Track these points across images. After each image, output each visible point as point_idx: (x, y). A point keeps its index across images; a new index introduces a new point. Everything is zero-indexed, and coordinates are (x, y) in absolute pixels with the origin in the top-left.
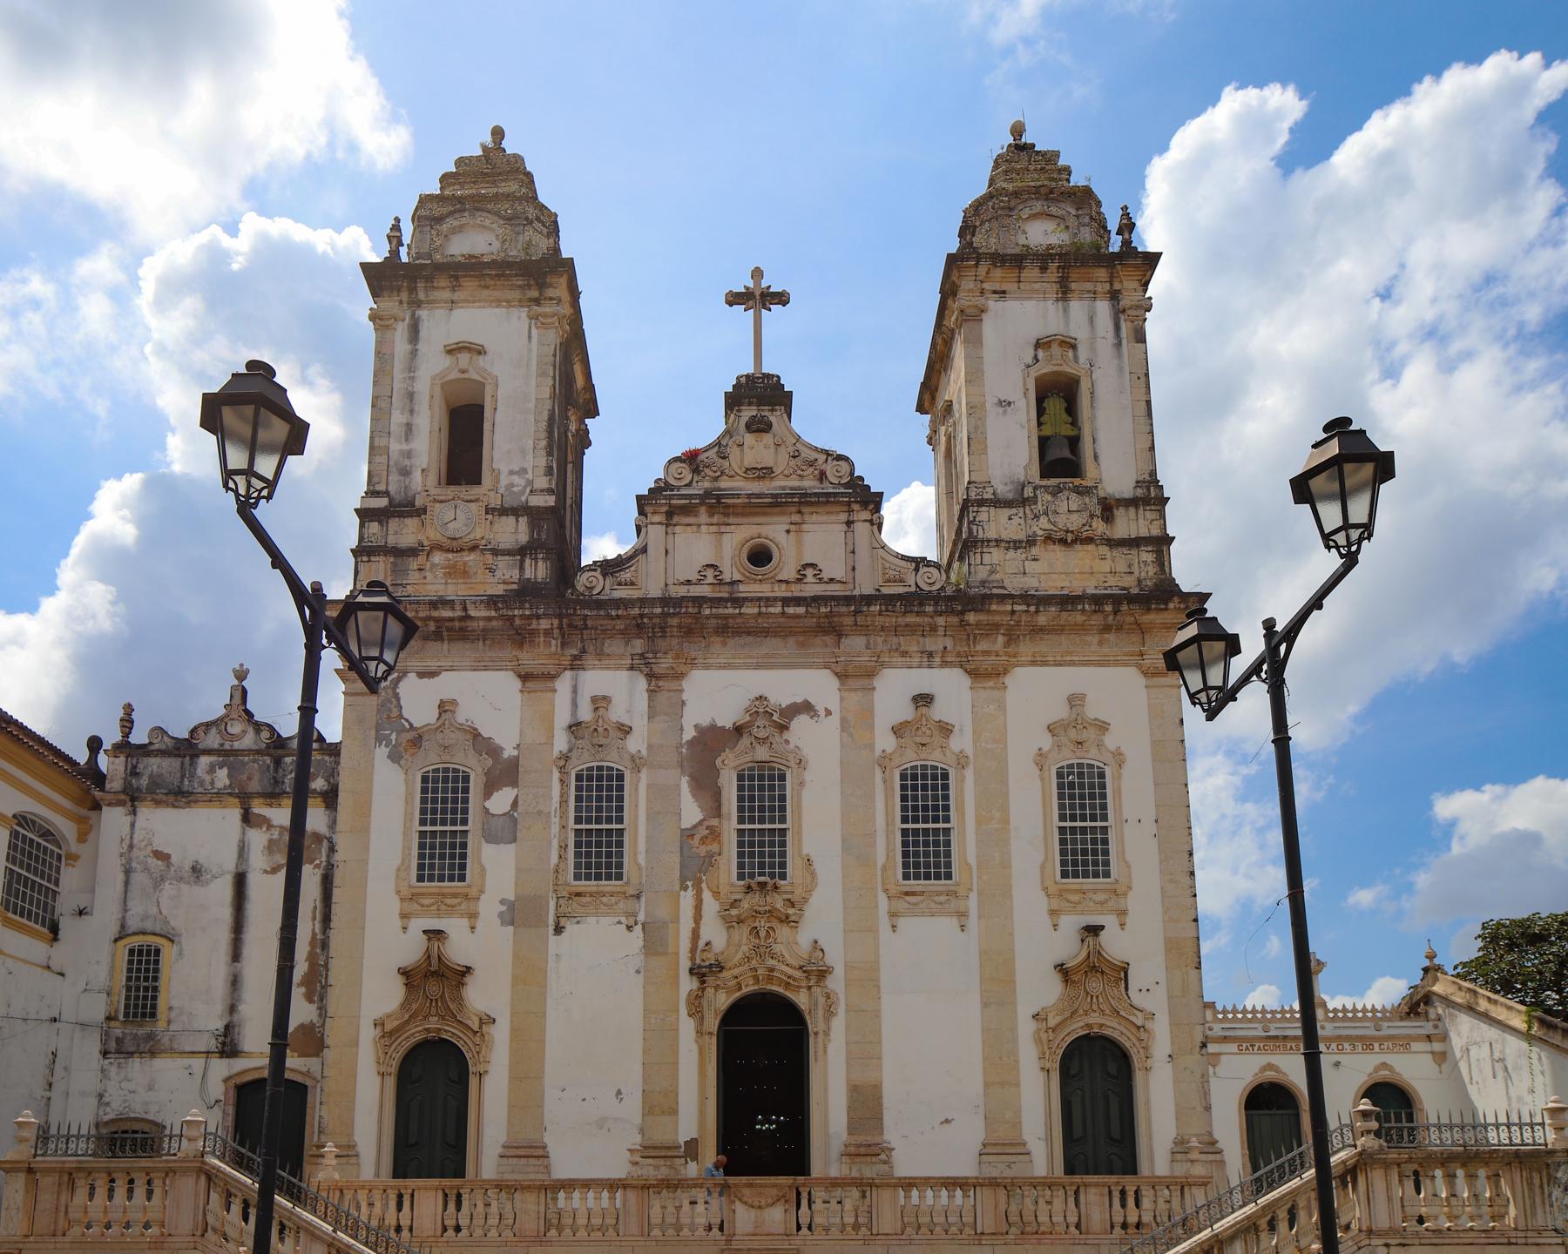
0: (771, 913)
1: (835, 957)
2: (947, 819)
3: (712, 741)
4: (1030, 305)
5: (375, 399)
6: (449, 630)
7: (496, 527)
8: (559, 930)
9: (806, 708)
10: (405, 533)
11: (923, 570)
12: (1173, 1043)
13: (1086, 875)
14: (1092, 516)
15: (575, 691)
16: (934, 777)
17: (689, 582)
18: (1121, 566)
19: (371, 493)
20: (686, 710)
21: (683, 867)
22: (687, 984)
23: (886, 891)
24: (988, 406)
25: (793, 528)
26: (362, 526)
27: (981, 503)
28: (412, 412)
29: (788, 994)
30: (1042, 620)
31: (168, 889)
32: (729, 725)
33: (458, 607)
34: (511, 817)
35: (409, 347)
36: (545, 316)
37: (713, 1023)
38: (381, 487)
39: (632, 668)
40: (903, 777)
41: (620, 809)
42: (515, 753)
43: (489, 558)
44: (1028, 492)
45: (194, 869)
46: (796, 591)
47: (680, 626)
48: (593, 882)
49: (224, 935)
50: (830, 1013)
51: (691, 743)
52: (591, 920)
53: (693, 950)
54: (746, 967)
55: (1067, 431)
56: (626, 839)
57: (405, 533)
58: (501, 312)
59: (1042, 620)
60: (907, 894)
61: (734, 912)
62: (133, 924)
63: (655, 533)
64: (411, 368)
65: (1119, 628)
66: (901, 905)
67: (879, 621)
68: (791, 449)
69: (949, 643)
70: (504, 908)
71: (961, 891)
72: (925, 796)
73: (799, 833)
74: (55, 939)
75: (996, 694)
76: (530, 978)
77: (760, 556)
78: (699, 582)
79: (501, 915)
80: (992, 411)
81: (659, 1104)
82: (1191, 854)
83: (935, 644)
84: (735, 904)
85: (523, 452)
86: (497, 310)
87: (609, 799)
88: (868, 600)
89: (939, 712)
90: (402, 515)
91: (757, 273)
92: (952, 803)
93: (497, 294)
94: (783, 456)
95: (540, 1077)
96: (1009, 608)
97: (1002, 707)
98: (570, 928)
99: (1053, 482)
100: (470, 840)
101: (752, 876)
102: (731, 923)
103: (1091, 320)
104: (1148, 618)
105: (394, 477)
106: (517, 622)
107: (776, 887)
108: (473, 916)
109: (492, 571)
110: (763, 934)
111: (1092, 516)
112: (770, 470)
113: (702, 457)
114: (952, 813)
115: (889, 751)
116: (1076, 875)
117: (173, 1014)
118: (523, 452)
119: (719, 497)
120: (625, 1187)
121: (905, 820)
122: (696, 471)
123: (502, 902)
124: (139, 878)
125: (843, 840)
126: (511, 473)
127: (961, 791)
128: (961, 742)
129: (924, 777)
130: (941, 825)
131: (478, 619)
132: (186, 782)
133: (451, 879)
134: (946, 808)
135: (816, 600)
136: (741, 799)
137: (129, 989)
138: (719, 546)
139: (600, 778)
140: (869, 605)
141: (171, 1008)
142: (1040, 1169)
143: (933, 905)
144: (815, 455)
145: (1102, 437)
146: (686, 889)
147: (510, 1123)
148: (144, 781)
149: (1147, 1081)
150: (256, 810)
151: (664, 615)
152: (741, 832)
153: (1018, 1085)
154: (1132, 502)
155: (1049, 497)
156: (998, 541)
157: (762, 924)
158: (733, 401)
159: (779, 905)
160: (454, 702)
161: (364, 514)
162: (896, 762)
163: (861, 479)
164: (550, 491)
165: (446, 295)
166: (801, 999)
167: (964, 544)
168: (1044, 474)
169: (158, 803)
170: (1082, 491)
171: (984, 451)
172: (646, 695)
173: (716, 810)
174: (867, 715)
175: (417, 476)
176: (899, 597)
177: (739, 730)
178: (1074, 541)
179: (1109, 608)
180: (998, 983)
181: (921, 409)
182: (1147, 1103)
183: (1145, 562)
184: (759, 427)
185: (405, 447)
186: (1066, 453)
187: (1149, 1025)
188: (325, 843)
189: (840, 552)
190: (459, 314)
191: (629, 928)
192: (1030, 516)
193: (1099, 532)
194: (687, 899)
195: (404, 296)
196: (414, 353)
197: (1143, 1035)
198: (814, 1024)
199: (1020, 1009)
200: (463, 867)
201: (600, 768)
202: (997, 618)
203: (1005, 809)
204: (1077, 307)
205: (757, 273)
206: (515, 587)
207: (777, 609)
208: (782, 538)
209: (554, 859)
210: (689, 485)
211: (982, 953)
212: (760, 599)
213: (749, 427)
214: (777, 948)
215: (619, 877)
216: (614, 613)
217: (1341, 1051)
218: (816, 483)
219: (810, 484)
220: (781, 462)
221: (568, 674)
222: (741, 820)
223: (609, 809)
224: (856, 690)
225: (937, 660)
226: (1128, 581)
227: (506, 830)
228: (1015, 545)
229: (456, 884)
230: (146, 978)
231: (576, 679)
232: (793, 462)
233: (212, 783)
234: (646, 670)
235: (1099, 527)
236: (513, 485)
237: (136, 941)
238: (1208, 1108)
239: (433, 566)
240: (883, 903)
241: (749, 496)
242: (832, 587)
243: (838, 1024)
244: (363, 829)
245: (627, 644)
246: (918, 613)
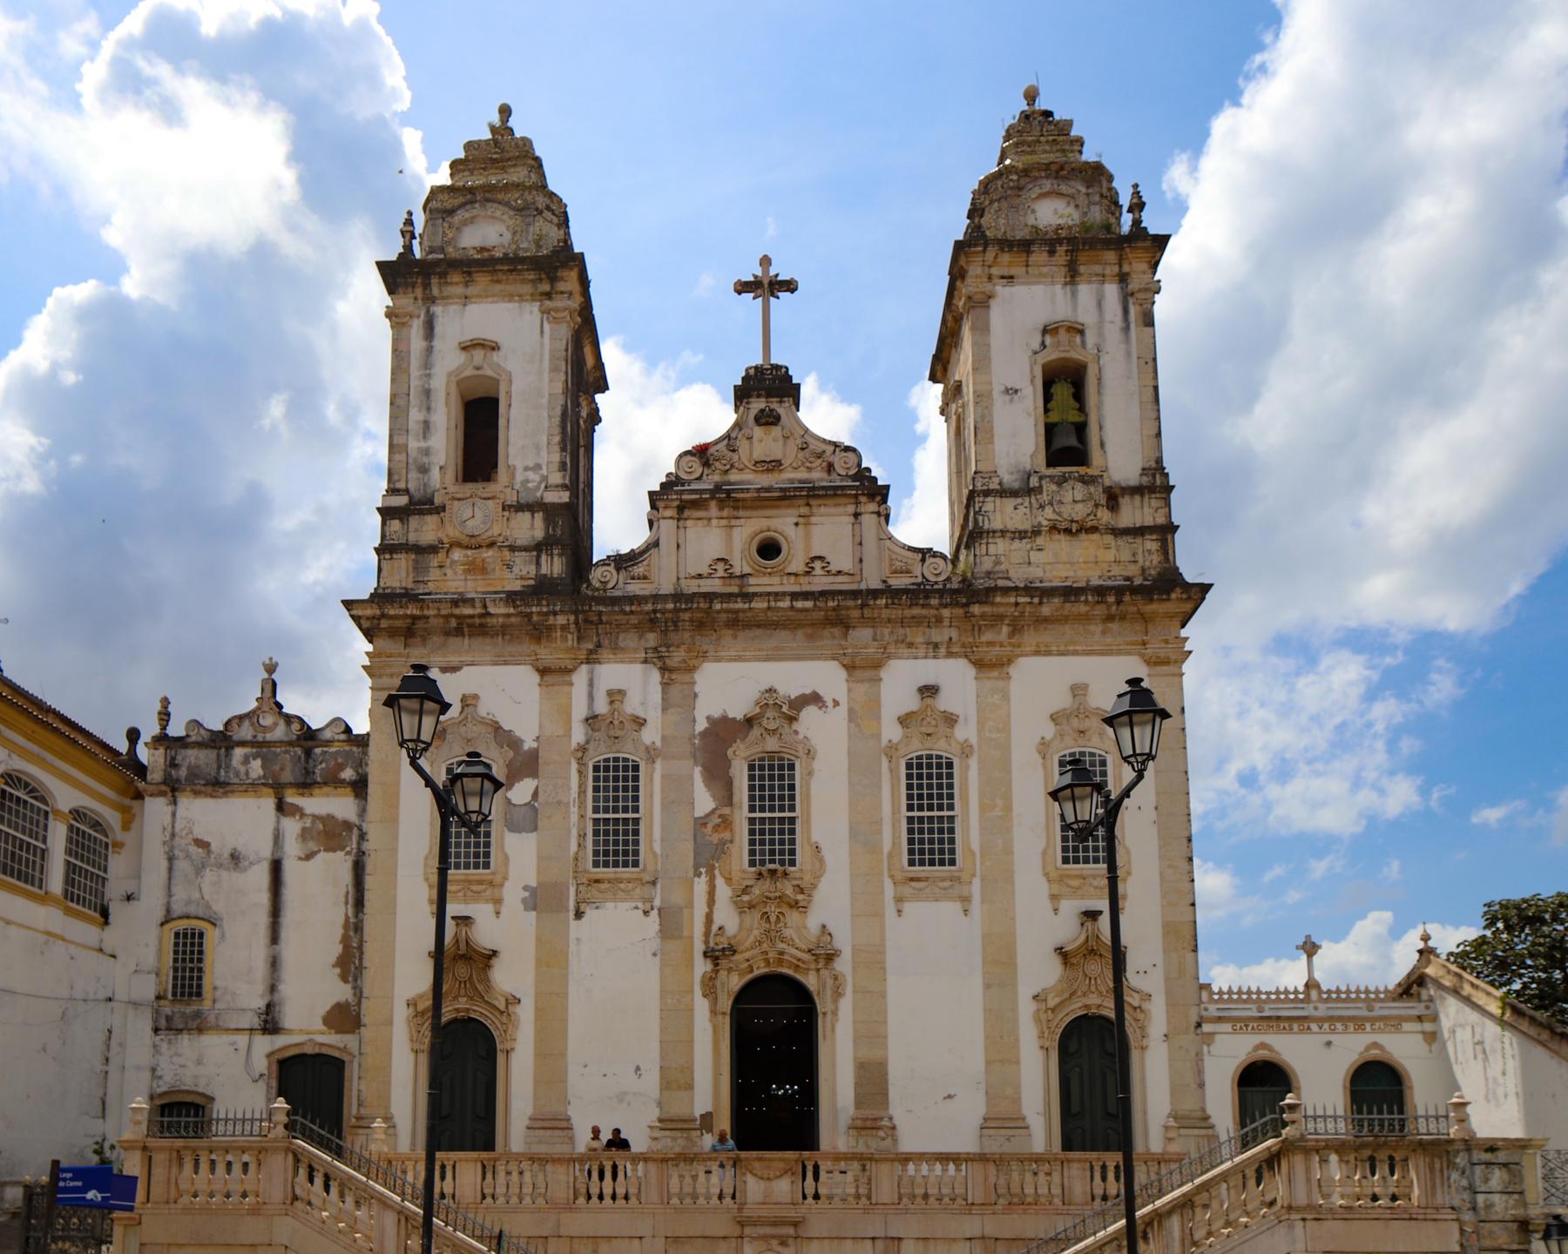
0: (781, 899)
1: (843, 941)
2: (951, 807)
3: (723, 732)
4: (1038, 290)
5: (394, 397)
6: (469, 626)
7: (513, 522)
8: (579, 915)
9: (815, 699)
10: (425, 530)
11: (929, 561)
12: (1169, 1022)
13: (1086, 861)
14: (1097, 506)
15: (591, 684)
16: (939, 766)
17: (700, 576)
18: (1126, 555)
19: (392, 491)
20: (699, 702)
21: (697, 854)
22: (702, 967)
23: (892, 877)
24: (996, 394)
25: (801, 520)
26: (384, 524)
27: (987, 493)
28: (429, 409)
29: (798, 977)
30: (1046, 610)
31: (209, 875)
32: (739, 716)
33: (478, 604)
34: (531, 807)
35: (424, 344)
36: (557, 310)
37: (726, 1004)
38: (401, 485)
39: (645, 661)
40: (909, 766)
41: (636, 799)
42: (535, 745)
43: (507, 553)
44: (1034, 482)
45: (232, 856)
46: (806, 585)
47: (691, 621)
48: (611, 869)
49: (263, 919)
50: (838, 994)
51: (704, 734)
52: (610, 905)
53: (707, 934)
54: (757, 951)
55: (1074, 417)
56: (642, 827)
57: (425, 530)
58: (513, 306)
59: (1046, 610)
60: (912, 879)
61: (746, 898)
62: (178, 909)
63: (667, 527)
64: (427, 364)
65: (1123, 618)
66: (907, 890)
67: (885, 613)
68: (799, 441)
69: (954, 634)
70: (527, 894)
71: (965, 876)
72: (930, 783)
73: (808, 821)
74: (106, 923)
75: (1001, 684)
76: (552, 961)
77: (769, 550)
78: (710, 576)
79: (524, 901)
80: (999, 400)
81: (676, 1079)
82: (1190, 840)
83: (940, 635)
84: (746, 890)
85: (538, 447)
86: (510, 305)
87: (625, 789)
89: (945, 702)
90: (421, 513)
91: (766, 261)
92: (956, 791)
93: (510, 288)
94: (792, 447)
95: (563, 1054)
96: (1012, 600)
97: (1006, 697)
98: (590, 913)
99: (1058, 471)
100: (494, 829)
101: (763, 863)
102: (744, 906)
103: (1100, 304)
104: (1149, 608)
105: (413, 475)
106: (535, 618)
107: (785, 874)
108: (498, 901)
109: (509, 567)
110: (773, 919)
111: (1097, 506)
112: (779, 463)
113: (712, 450)
114: (957, 801)
115: (895, 740)
116: (1076, 861)
117: (218, 993)
118: (538, 447)
119: (728, 492)
120: (646, 1160)
121: (910, 808)
122: (706, 464)
123: (526, 888)
124: (182, 865)
125: (851, 828)
126: (526, 469)
127: (965, 779)
128: (966, 731)
129: (929, 766)
130: (946, 813)
131: (498, 616)
132: (222, 773)
133: (476, 866)
135: (824, 594)
136: (752, 788)
137: (176, 970)
138: (729, 540)
139: (616, 769)
140: (875, 598)
141: (215, 988)
142: (1038, 1144)
143: (937, 890)
145: (1109, 424)
146: (699, 875)
147: (536, 1098)
148: (183, 773)
149: (1143, 1059)
150: (289, 800)
151: (676, 611)
152: (752, 821)
153: (1018, 1063)
154: (1138, 490)
155: (1054, 487)
156: (1003, 533)
157: (772, 909)
158: (742, 394)
159: (789, 891)
160: (476, 697)
161: (386, 513)
163: (869, 470)
164: (564, 487)
165: (459, 290)
166: (810, 981)
167: (970, 534)
168: (1050, 464)
169: (197, 793)
170: (1087, 481)
172: (659, 688)
173: (727, 798)
174: (874, 705)
175: (435, 473)
176: (906, 591)
177: (749, 722)
178: (1079, 531)
179: (1111, 599)
180: (1000, 964)
181: (933, 378)
182: (1143, 1080)
183: (1149, 551)
184: (768, 419)
185: (422, 444)
186: (1073, 442)
187: (1145, 1006)
188: (355, 831)
189: (847, 544)
190: (474, 309)
191: (646, 913)
192: (1035, 505)
193: (1104, 521)
194: (701, 885)
195: (419, 292)
196: (429, 350)
197: (1140, 1016)
198: (823, 1004)
199: (1021, 989)
200: (487, 855)
201: (616, 760)
202: (1001, 610)
204: (1085, 291)
205: (766, 261)
206: (532, 582)
207: (785, 604)
208: (791, 531)
209: (574, 847)
210: (699, 478)
211: (985, 936)
213: (758, 420)
214: (788, 932)
215: (636, 864)
216: (627, 609)
217: (1333, 1031)
218: (825, 475)
219: (818, 476)
220: (790, 454)
221: (584, 668)
222: (752, 809)
223: (625, 799)
224: (863, 681)
225: (943, 650)
226: (1133, 570)
227: (528, 819)
228: (1021, 535)
229: (481, 871)
230: (192, 961)
231: (591, 672)
232: (801, 455)
233: (247, 774)
234: (660, 664)
235: (1104, 516)
236: (528, 481)
237: (181, 925)
238: (1202, 1085)
239: (453, 562)
240: (889, 889)
241: (758, 490)
242: (840, 579)
243: (846, 1004)
244: (392, 820)
245: (640, 638)
246: (923, 606)
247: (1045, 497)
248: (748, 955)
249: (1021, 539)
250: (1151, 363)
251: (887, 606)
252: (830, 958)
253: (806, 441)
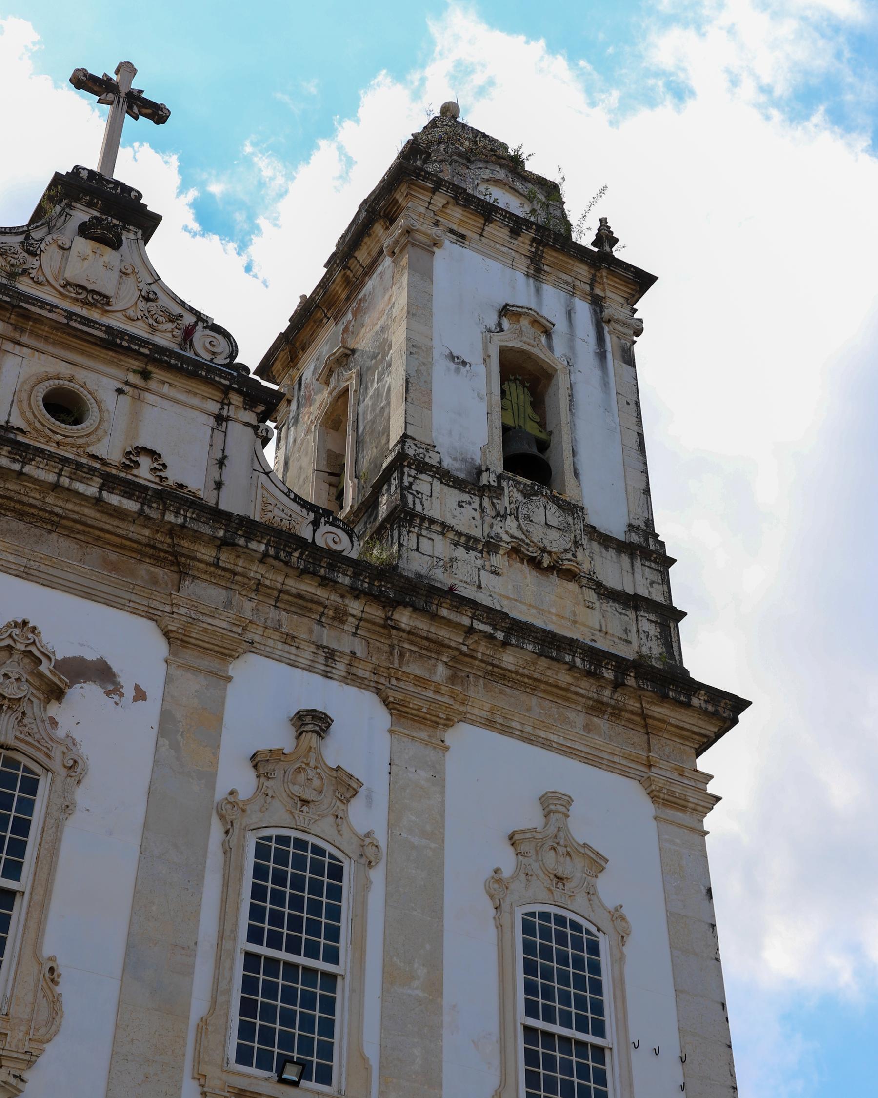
4: (494, 266)
9: (101, 673)
11: (324, 528)
27: (422, 467)
30: (509, 659)
40: (262, 851)
68: (145, 288)
69: (360, 649)
72: (296, 896)
77: (65, 406)
80: (441, 370)
88: (249, 527)
89: (336, 751)
92: (344, 925)
97: (438, 778)
104: (660, 711)
121: (254, 935)
125: (130, 947)
128: (367, 816)
129: (300, 862)
130: (320, 965)
134: (334, 934)
140: (248, 538)
144: (177, 310)
155: (520, 497)
156: (445, 528)
162: (254, 818)
168: (506, 467)
171: (428, 405)
174: (210, 721)
178: (551, 569)
193: (586, 567)
202: (443, 633)
203: (435, 963)
212: (65, 461)
220: (126, 297)
224: (197, 670)
228: (469, 543)
246: (325, 582)
247: (504, 503)
249: (468, 549)
250: (632, 405)
251: (264, 558)
253: (153, 291)
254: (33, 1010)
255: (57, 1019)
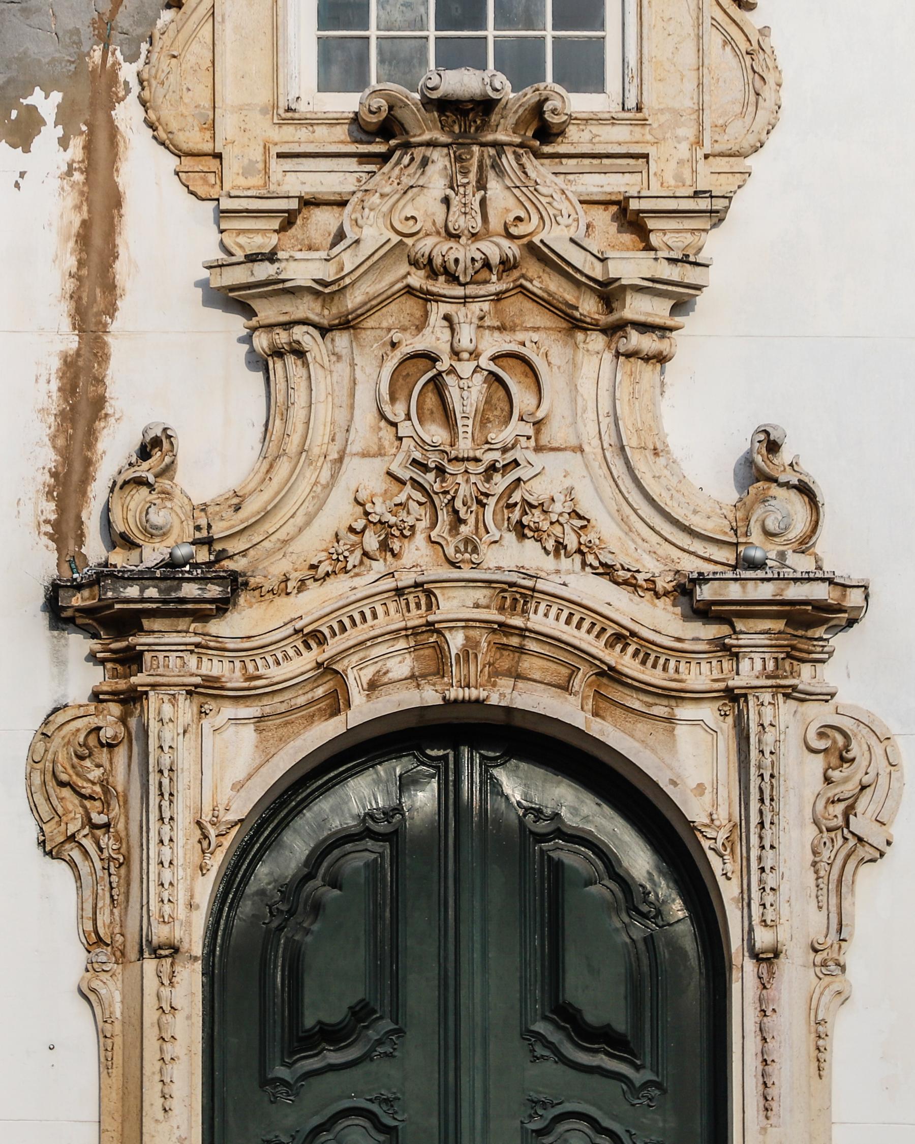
29: (612, 733)
107: (543, 130)
248: (311, 604)
252: (812, 621)
254: (700, 85)
255: (767, 92)
